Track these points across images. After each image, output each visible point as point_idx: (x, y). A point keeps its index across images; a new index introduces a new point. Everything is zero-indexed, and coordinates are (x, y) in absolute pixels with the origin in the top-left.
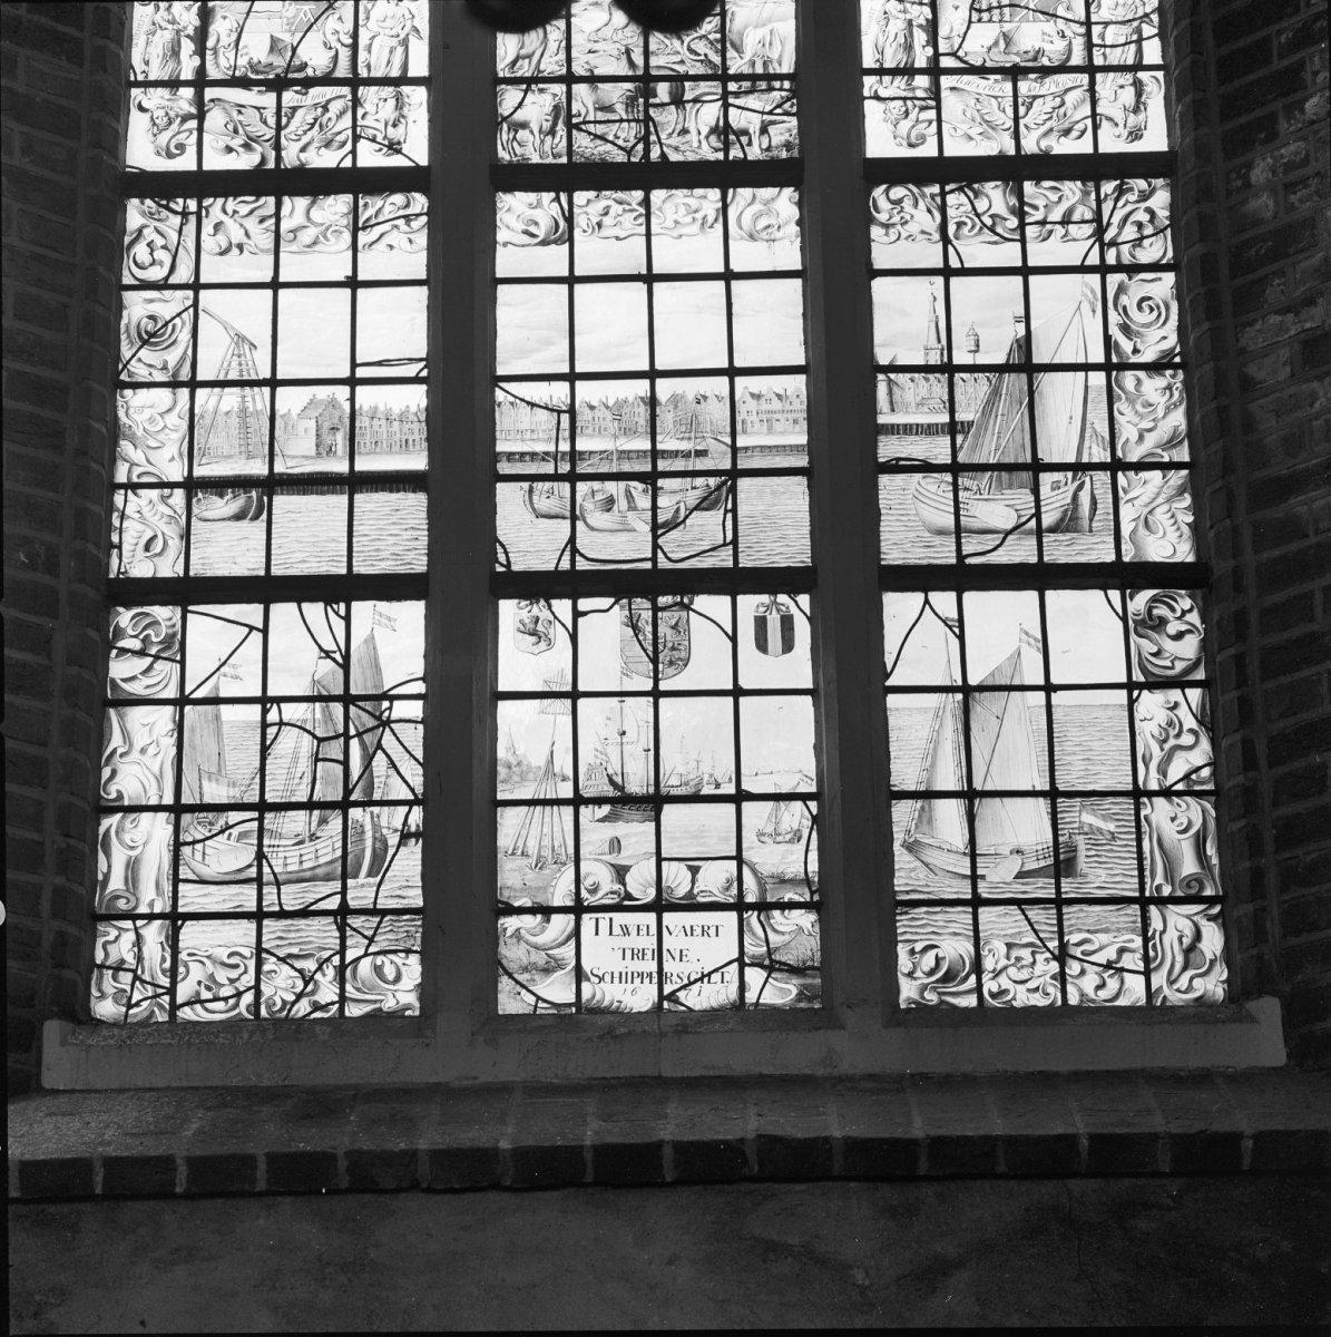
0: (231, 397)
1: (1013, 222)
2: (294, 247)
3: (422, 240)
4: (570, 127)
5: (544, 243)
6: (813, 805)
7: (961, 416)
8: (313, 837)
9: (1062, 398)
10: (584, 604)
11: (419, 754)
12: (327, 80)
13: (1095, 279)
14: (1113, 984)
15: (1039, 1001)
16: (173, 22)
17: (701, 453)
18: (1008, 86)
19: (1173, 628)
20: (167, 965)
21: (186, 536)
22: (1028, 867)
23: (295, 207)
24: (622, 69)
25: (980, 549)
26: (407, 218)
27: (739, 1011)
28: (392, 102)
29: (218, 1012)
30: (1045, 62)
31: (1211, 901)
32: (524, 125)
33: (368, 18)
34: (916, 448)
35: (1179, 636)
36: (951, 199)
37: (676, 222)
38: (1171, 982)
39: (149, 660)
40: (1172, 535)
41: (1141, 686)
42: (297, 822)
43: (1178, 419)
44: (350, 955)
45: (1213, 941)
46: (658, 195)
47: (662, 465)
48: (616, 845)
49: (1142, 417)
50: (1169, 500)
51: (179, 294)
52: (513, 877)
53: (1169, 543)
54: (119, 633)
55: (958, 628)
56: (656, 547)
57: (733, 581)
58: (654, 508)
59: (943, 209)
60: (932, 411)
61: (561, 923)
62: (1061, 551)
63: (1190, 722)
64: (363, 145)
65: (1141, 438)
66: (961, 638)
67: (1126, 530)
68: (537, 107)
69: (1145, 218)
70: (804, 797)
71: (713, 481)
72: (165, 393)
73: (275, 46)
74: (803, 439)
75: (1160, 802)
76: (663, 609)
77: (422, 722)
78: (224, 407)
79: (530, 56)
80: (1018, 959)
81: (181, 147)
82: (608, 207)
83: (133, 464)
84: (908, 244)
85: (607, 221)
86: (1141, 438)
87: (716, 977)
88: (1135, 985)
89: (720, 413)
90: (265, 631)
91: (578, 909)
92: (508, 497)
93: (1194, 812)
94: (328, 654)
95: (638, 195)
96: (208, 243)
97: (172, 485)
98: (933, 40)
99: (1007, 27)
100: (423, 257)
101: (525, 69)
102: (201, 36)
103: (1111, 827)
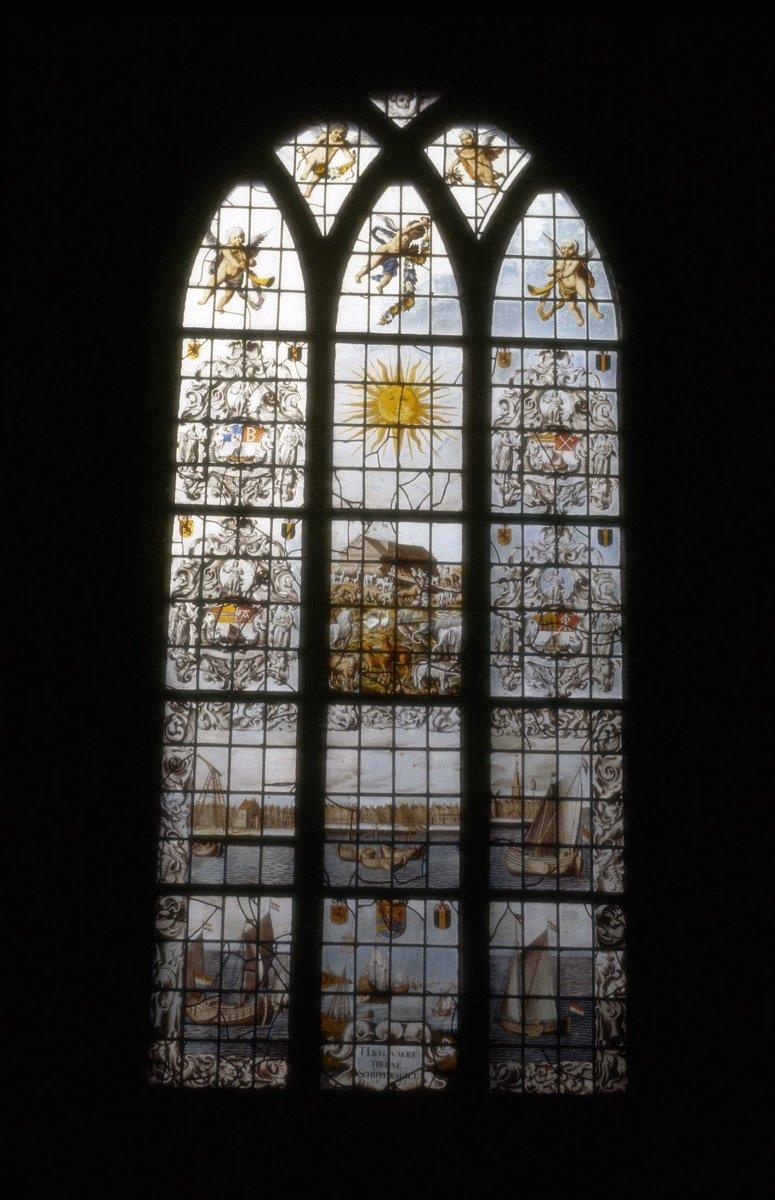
0: (209, 799)
1: (553, 729)
2: (238, 728)
3: (295, 726)
4: (361, 674)
5: (349, 729)
6: (456, 999)
7: (530, 820)
8: (242, 1005)
9: (572, 813)
10: (361, 902)
11: (288, 969)
12: (254, 646)
13: (587, 757)
14: (579, 1085)
15: (548, 1091)
16: (187, 616)
17: (413, 833)
18: (554, 662)
19: (614, 922)
20: (180, 1061)
21: (189, 862)
22: (548, 1030)
23: (239, 709)
24: (385, 648)
25: (532, 882)
26: (289, 716)
27: (421, 1092)
28: (282, 659)
29: (199, 1084)
30: (570, 651)
31: (622, 1049)
32: (341, 672)
33: (273, 617)
34: (507, 835)
35: (615, 927)
36: (527, 716)
37: (406, 722)
38: (604, 1084)
39: (173, 921)
40: (615, 880)
41: (598, 949)
42: (237, 998)
43: (620, 825)
44: (258, 1060)
45: (622, 1067)
46: (399, 709)
47: (396, 838)
48: (371, 1014)
49: (604, 823)
50: (615, 863)
51: (188, 748)
52: (325, 1024)
53: (613, 885)
54: (161, 908)
55: (521, 918)
56: (393, 876)
57: (425, 894)
58: (392, 858)
59: (523, 723)
60: (515, 817)
61: (346, 1049)
62: (568, 886)
63: (618, 967)
64: (270, 679)
65: (604, 833)
66: (522, 924)
67: (596, 875)
68: (346, 664)
69: (609, 728)
70: (452, 996)
71: (418, 847)
72: (179, 797)
73: (233, 630)
74: (457, 828)
75: (604, 1003)
76: (395, 905)
77: (290, 954)
78: (207, 803)
79: (344, 639)
80: (540, 1072)
81: (190, 677)
82: (376, 714)
83: (167, 829)
84: (506, 737)
85: (376, 720)
86: (604, 833)
87: (412, 1076)
88: (589, 1085)
89: (421, 814)
90: (223, 909)
91: (354, 1042)
92: (329, 848)
93: (618, 1008)
94: (249, 921)
95: (390, 708)
96: (201, 724)
97: (183, 839)
98: (521, 639)
99: (555, 633)
100: (294, 735)
101: (342, 646)
102: (199, 623)
103: (582, 1013)
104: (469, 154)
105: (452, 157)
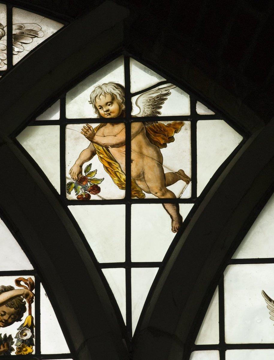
104: (113, 134)
105: (77, 143)
